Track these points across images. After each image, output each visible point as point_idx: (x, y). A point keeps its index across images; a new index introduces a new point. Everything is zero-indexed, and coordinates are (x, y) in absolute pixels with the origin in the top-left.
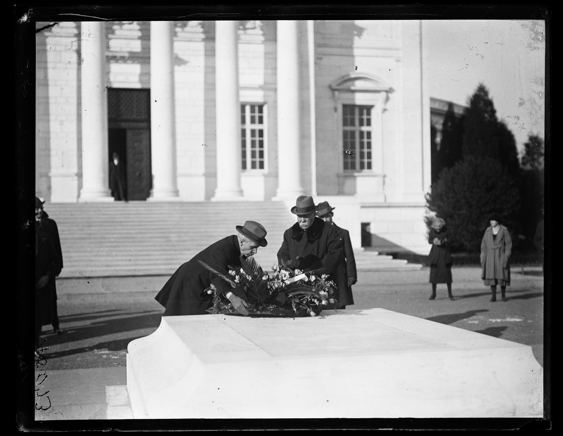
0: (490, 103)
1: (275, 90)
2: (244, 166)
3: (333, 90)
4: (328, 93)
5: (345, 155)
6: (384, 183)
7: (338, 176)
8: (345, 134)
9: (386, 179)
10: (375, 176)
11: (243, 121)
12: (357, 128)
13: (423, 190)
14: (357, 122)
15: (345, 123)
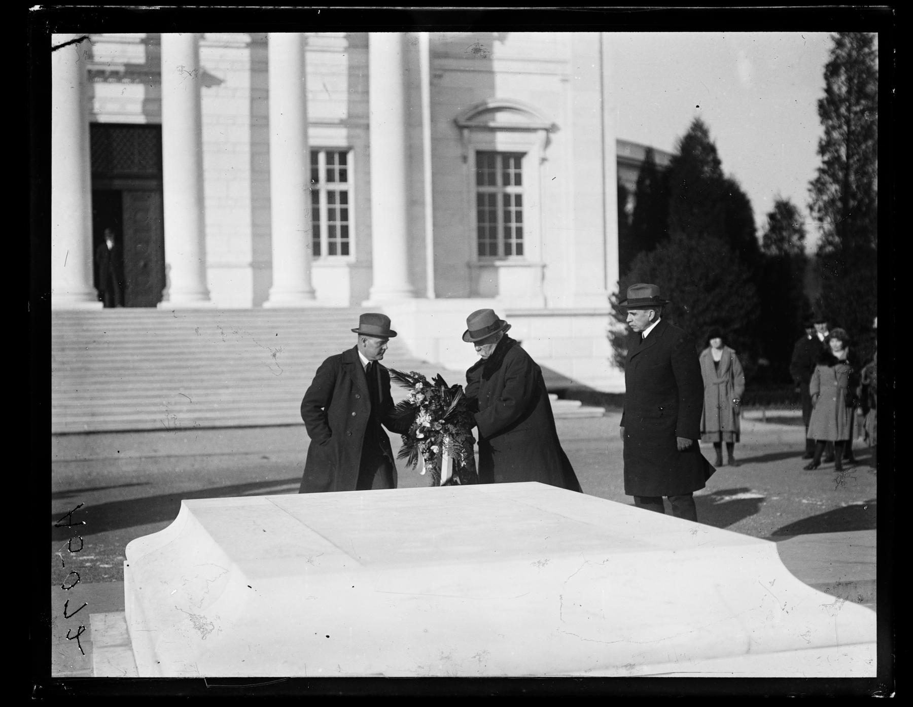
0: (712, 149)
1: (367, 127)
2: (316, 251)
3: (461, 128)
4: (452, 132)
5: (481, 232)
6: (543, 277)
7: (469, 266)
8: (480, 197)
9: (547, 271)
10: (529, 266)
11: (315, 178)
12: (499, 189)
13: (606, 288)
14: (499, 180)
15: (480, 181)
